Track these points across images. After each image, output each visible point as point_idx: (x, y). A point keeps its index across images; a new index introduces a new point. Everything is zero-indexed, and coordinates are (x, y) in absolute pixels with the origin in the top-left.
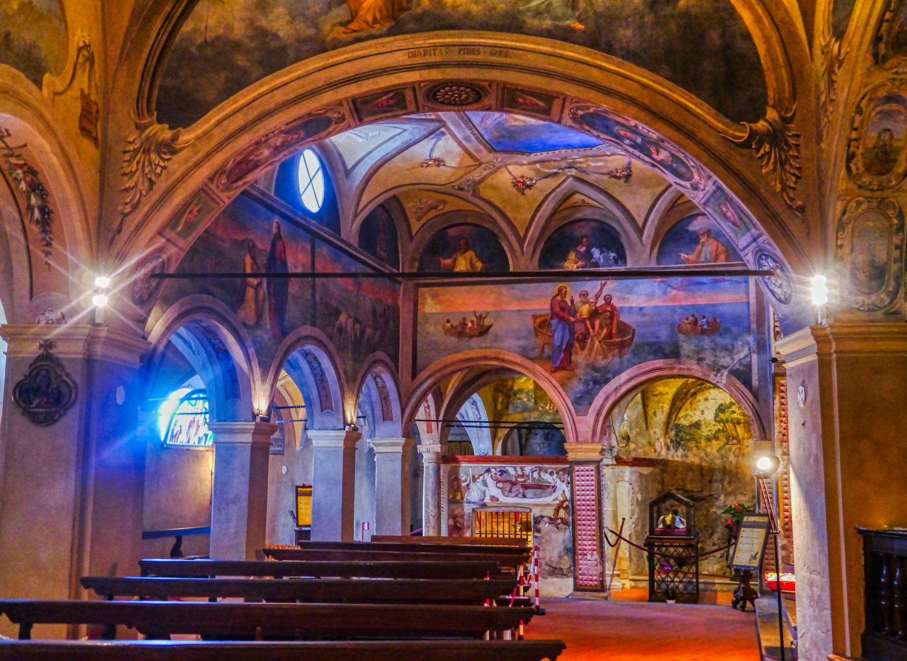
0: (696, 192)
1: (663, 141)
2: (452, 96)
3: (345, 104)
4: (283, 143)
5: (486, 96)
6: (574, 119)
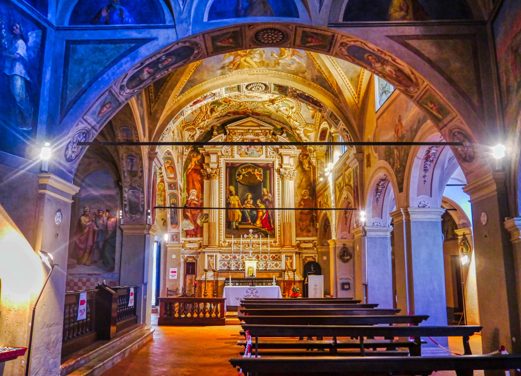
0: (119, 87)
1: (153, 79)
2: (273, 36)
3: (334, 53)
4: (377, 62)
5: (252, 38)
6: (196, 44)
